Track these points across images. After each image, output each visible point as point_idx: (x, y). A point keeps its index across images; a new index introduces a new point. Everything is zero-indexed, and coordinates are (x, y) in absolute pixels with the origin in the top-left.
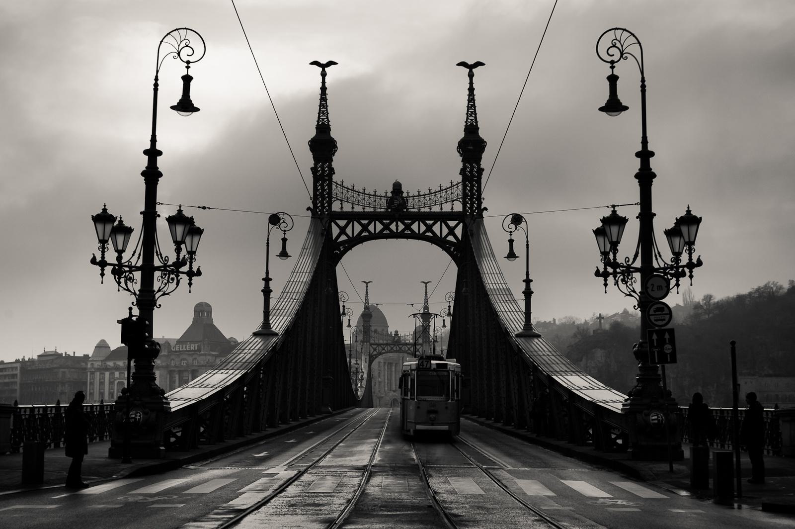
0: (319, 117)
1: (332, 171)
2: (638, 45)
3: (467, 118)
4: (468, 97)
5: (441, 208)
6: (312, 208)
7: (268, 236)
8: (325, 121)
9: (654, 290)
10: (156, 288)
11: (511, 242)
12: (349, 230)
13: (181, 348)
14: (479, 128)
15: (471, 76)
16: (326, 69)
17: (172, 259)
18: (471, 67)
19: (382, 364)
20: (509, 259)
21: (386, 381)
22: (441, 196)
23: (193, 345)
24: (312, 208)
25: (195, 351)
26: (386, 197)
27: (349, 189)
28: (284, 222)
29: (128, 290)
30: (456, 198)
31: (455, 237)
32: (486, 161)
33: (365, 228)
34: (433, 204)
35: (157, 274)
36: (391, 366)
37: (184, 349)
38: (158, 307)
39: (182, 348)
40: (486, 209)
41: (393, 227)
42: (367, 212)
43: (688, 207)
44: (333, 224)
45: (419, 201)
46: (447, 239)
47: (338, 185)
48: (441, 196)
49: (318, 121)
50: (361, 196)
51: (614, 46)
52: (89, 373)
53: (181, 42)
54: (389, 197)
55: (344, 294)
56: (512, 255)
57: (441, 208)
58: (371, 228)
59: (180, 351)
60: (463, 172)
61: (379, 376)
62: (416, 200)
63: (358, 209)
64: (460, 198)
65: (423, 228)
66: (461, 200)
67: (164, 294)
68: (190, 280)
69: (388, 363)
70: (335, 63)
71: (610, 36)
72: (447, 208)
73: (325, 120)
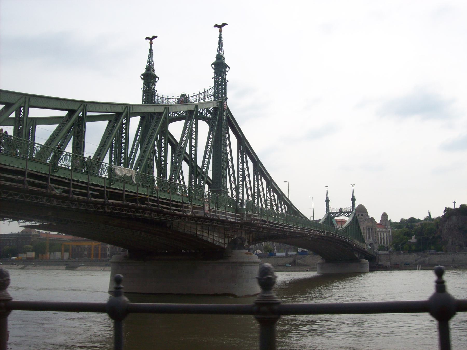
19: (365, 228)
21: (367, 235)
27: (161, 97)
30: (212, 95)
36: (370, 229)
48: (205, 95)
61: (364, 233)
62: (192, 98)
69: (368, 228)
70: (156, 37)
72: (207, 100)
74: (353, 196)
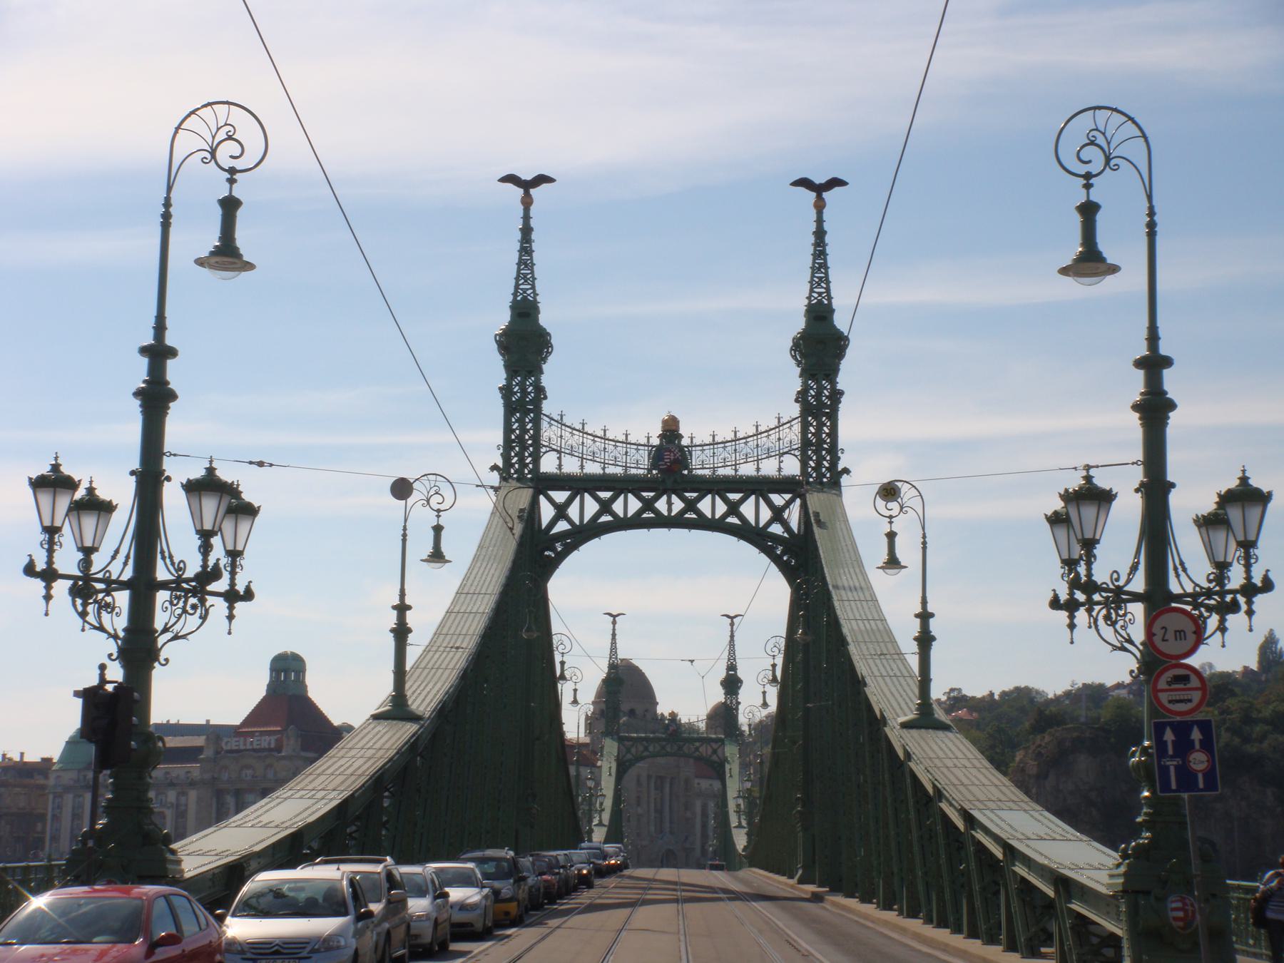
0: (517, 287)
1: (540, 392)
2: (1142, 139)
3: (812, 291)
4: (812, 248)
5: (758, 469)
6: (501, 466)
7: (406, 521)
8: (529, 295)
9: (1167, 640)
10: (159, 624)
11: (891, 536)
12: (573, 511)
13: (241, 743)
14: (834, 310)
15: (820, 206)
16: (532, 191)
17: (193, 569)
18: (819, 189)
20: (887, 571)
22: (757, 445)
23: (267, 738)
24: (501, 466)
25: (270, 750)
26: (648, 446)
27: (574, 429)
28: (437, 493)
29: (101, 628)
31: (785, 524)
32: (848, 375)
33: (605, 507)
34: (742, 461)
35: (162, 596)
37: (249, 747)
38: (164, 662)
39: (245, 745)
40: (846, 471)
41: (661, 505)
42: (609, 475)
43: (1244, 471)
44: (542, 498)
45: (714, 453)
46: (769, 530)
47: (552, 422)
48: (757, 445)
49: (515, 294)
50: (599, 444)
51: (1092, 143)
52: (51, 797)
53: (218, 129)
54: (654, 446)
55: (564, 638)
56: (893, 562)
57: (758, 469)
58: (618, 507)
59: (238, 751)
60: (802, 397)
61: (639, 804)
62: (708, 452)
63: (593, 468)
64: (797, 449)
65: (721, 508)
66: (797, 453)
67: (176, 637)
68: (231, 608)
71: (1085, 121)
72: (769, 468)
73: (529, 292)
74: (732, 667)
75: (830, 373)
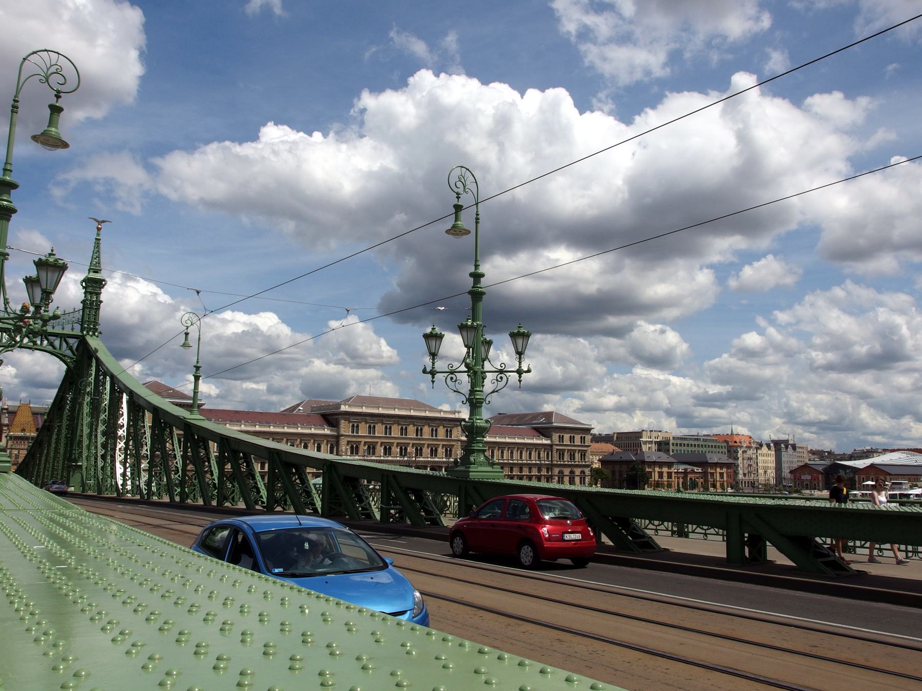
18: (100, 222)
60: (83, 302)
66: (80, 323)
75: (98, 294)
